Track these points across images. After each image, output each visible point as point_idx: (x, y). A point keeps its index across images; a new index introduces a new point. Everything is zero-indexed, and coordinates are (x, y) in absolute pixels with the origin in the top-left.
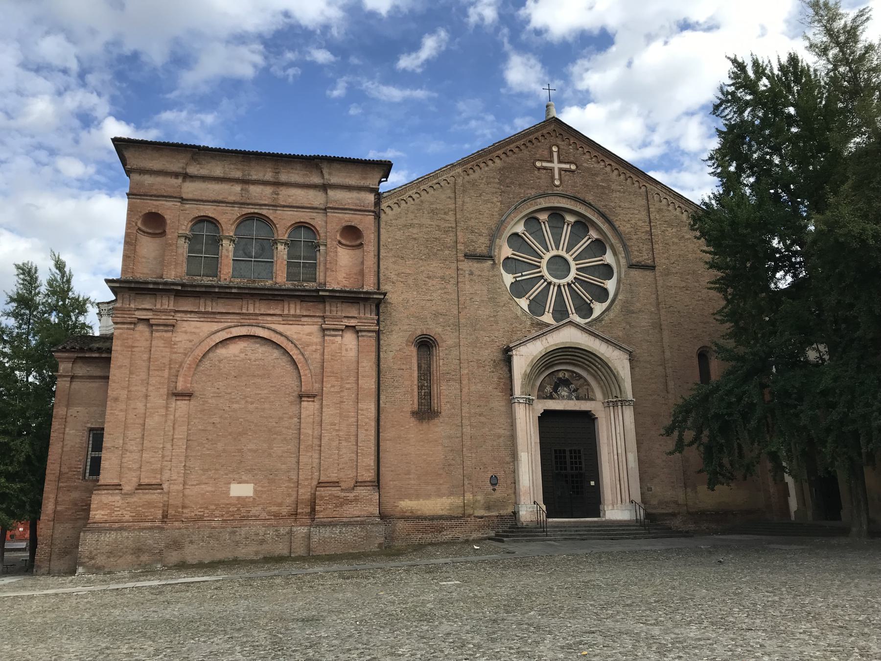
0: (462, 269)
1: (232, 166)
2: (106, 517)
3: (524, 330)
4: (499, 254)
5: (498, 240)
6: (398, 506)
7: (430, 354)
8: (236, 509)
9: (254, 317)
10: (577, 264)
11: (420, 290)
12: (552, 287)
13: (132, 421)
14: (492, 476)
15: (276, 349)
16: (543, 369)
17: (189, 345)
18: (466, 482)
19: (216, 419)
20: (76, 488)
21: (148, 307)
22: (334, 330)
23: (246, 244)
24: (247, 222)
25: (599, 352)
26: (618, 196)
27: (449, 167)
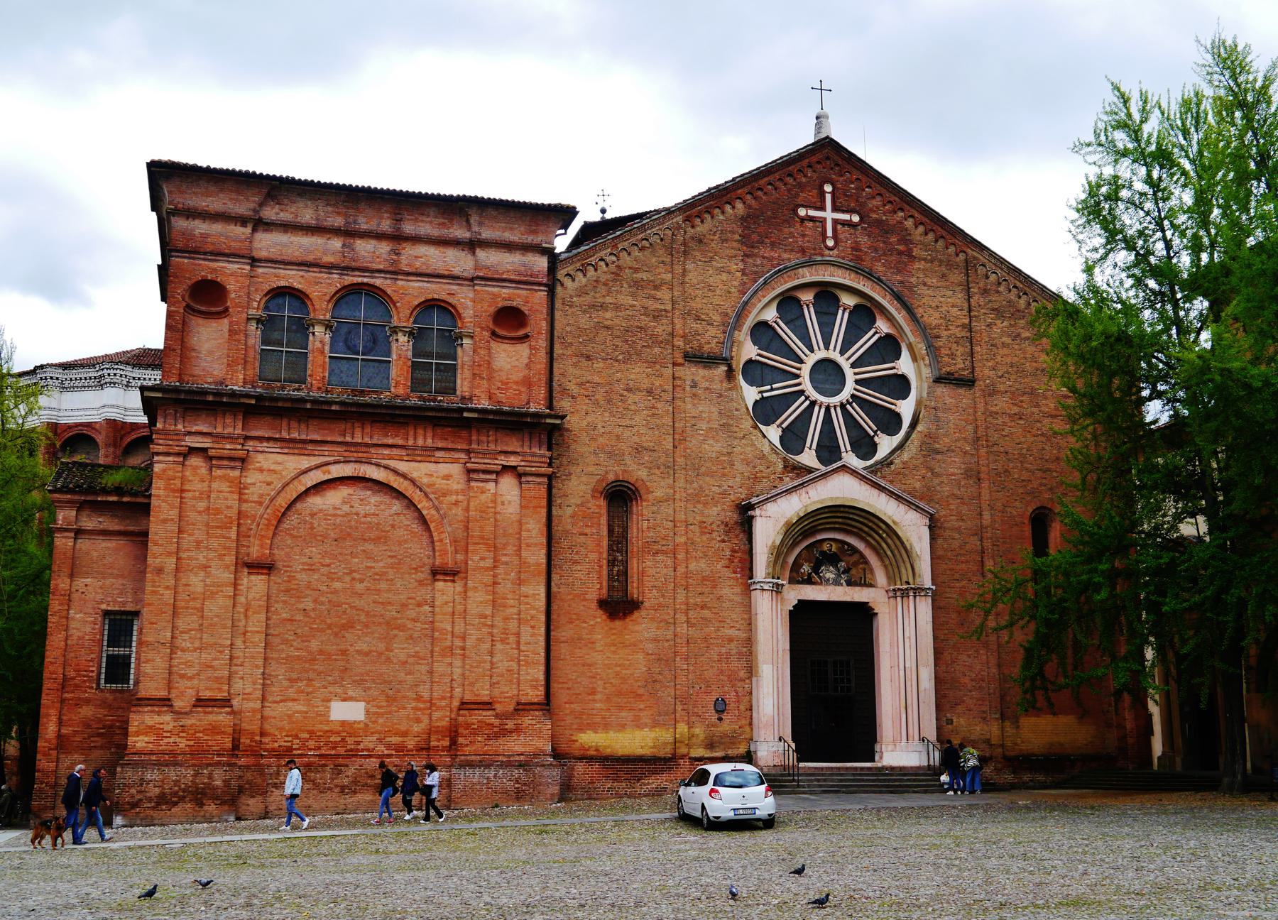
0: (680, 378)
1: (330, 209)
2: (151, 745)
3: (773, 476)
4: (739, 355)
7: (626, 511)
8: (339, 739)
10: (855, 374)
11: (615, 409)
12: (817, 408)
13: (183, 604)
17: (265, 489)
18: (679, 708)
19: (310, 606)
20: (88, 701)
21: (205, 430)
23: (350, 332)
24: (351, 297)
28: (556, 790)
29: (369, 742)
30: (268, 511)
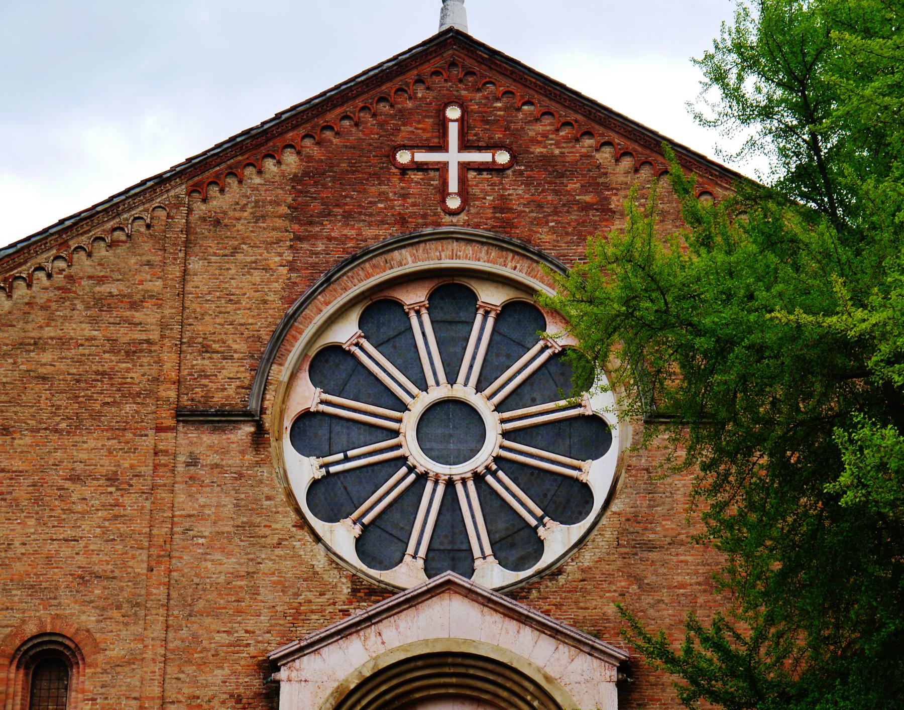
0: (166, 453)
3: (330, 609)
5: (274, 367)
7: (66, 688)
10: (503, 421)
12: (429, 486)
27: (149, 184)
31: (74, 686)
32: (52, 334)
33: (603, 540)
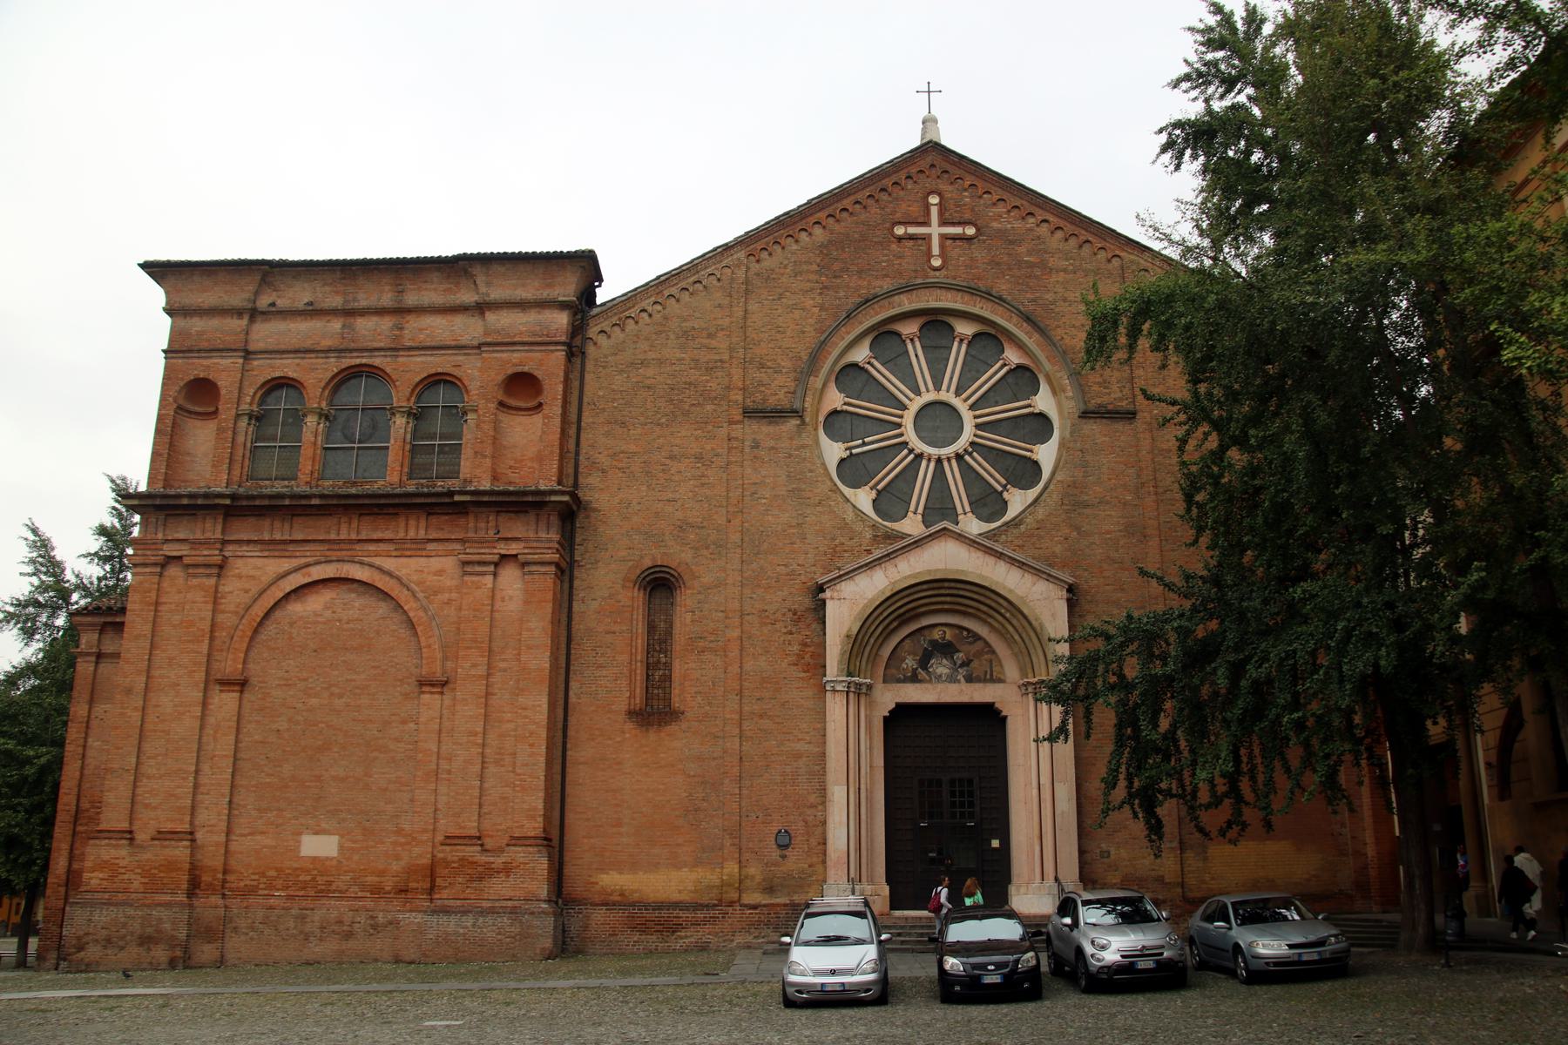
1: (327, 289)
2: (105, 882)
5: (812, 378)
6: (597, 883)
7: (672, 604)
8: (309, 878)
9: (348, 547)
10: (975, 417)
11: (654, 482)
12: (924, 463)
14: (780, 831)
15: (385, 600)
16: (895, 624)
22: (480, 563)
25: (1005, 588)
26: (1060, 279)
27: (719, 250)
28: (547, 943)
29: (342, 881)
30: (244, 621)
31: (678, 603)
32: (654, 356)
33: (1053, 499)
